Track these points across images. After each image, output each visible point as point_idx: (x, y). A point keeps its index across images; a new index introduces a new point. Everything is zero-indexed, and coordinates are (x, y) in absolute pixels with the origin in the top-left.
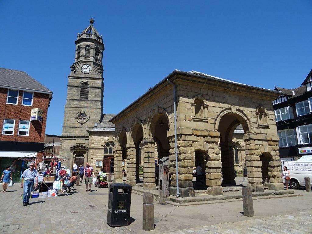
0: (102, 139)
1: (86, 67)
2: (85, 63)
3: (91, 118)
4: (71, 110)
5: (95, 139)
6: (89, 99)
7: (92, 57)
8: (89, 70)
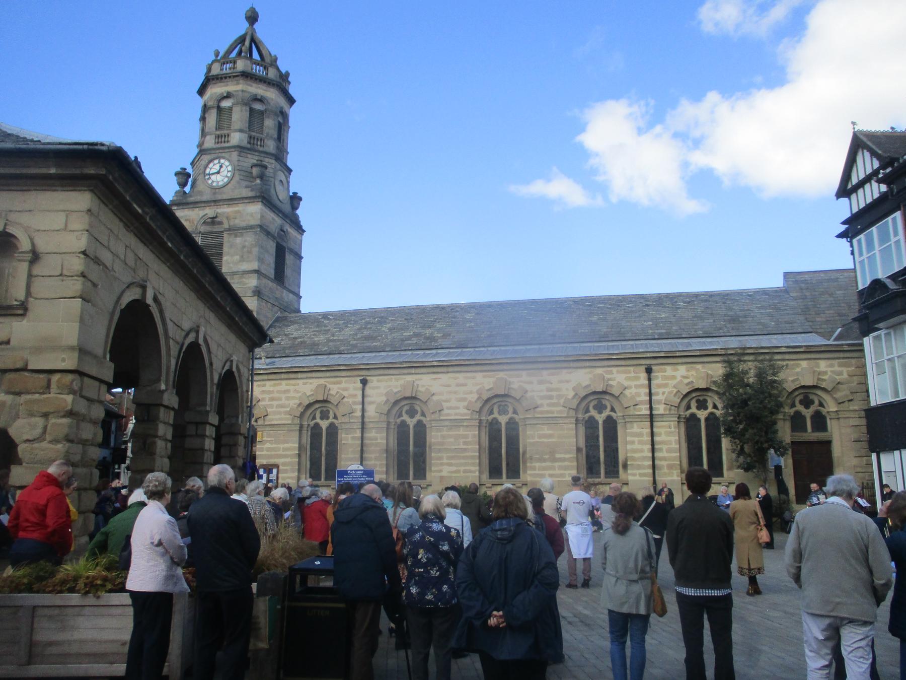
1: (217, 167)
2: (215, 156)
7: (236, 131)
8: (227, 176)
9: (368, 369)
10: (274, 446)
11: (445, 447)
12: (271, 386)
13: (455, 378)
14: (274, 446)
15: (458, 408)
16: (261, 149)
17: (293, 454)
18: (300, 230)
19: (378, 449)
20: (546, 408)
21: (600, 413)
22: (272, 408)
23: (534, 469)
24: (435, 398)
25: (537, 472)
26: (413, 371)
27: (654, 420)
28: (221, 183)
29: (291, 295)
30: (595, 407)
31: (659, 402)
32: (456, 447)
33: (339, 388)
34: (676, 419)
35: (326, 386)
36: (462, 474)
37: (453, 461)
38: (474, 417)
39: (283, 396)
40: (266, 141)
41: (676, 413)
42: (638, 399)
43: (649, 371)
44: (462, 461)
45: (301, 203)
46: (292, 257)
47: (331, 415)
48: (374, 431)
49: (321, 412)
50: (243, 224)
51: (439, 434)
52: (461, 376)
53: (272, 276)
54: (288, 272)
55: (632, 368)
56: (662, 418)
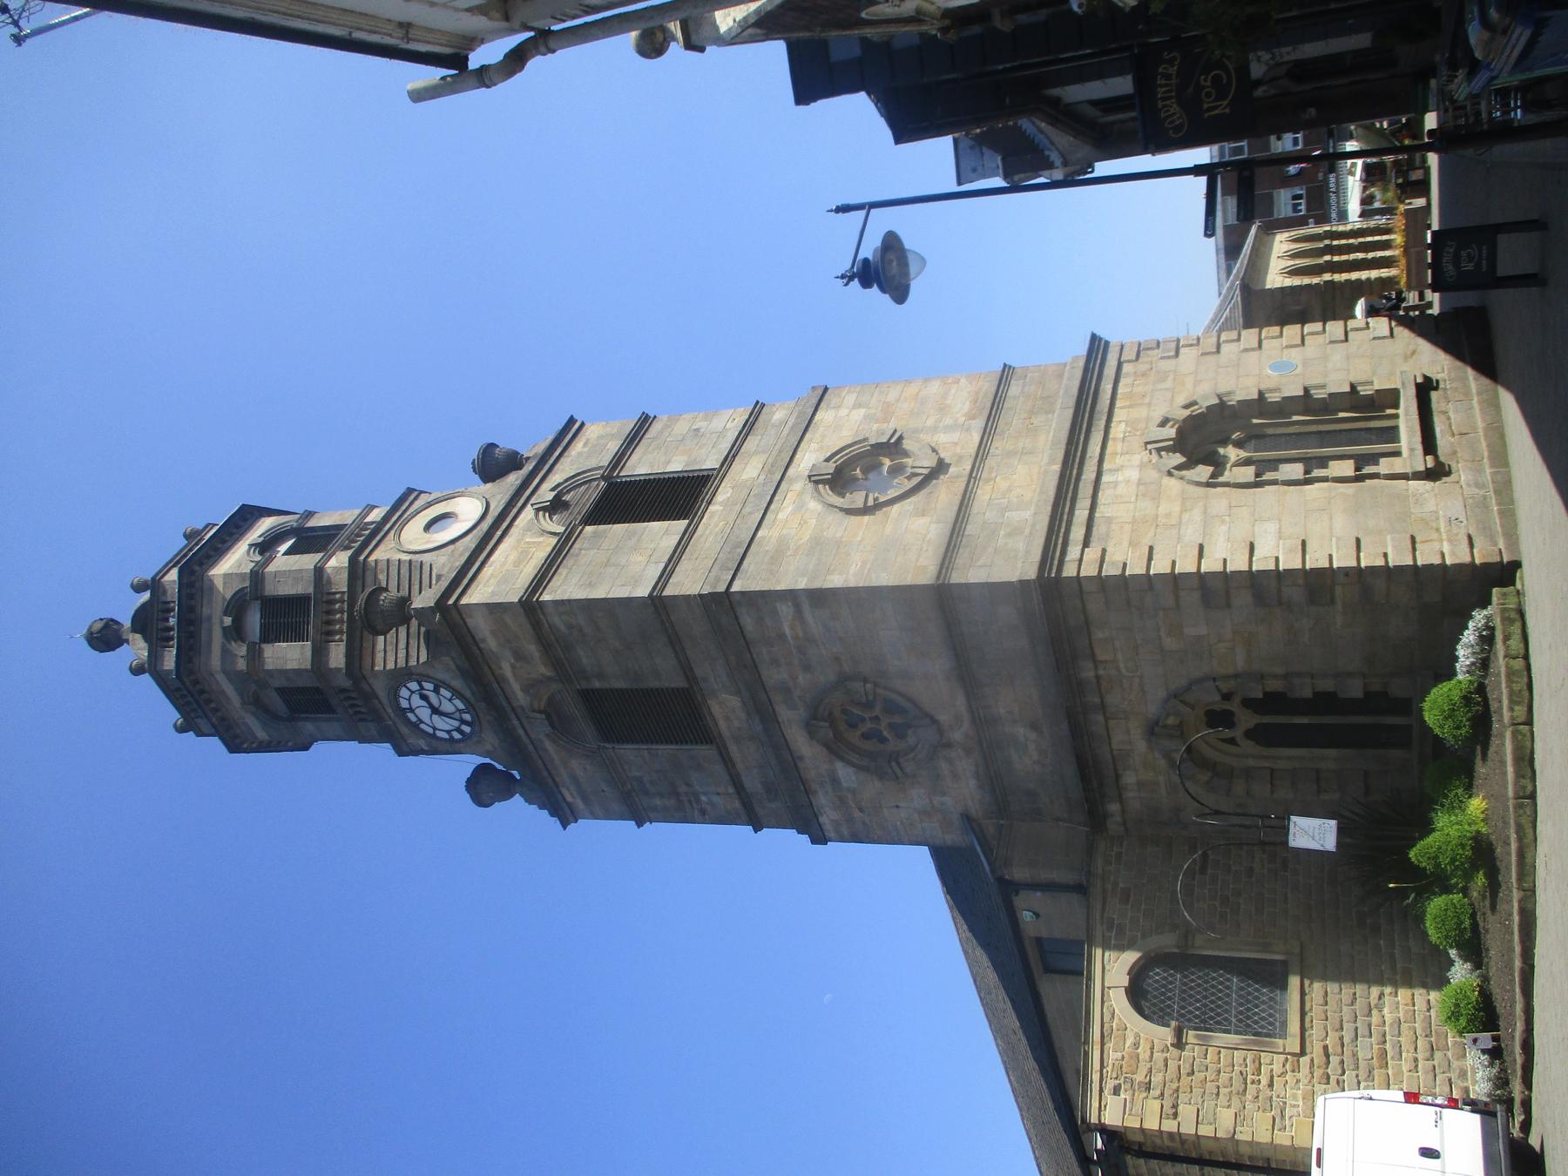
46: (635, 457)
53: (683, 523)
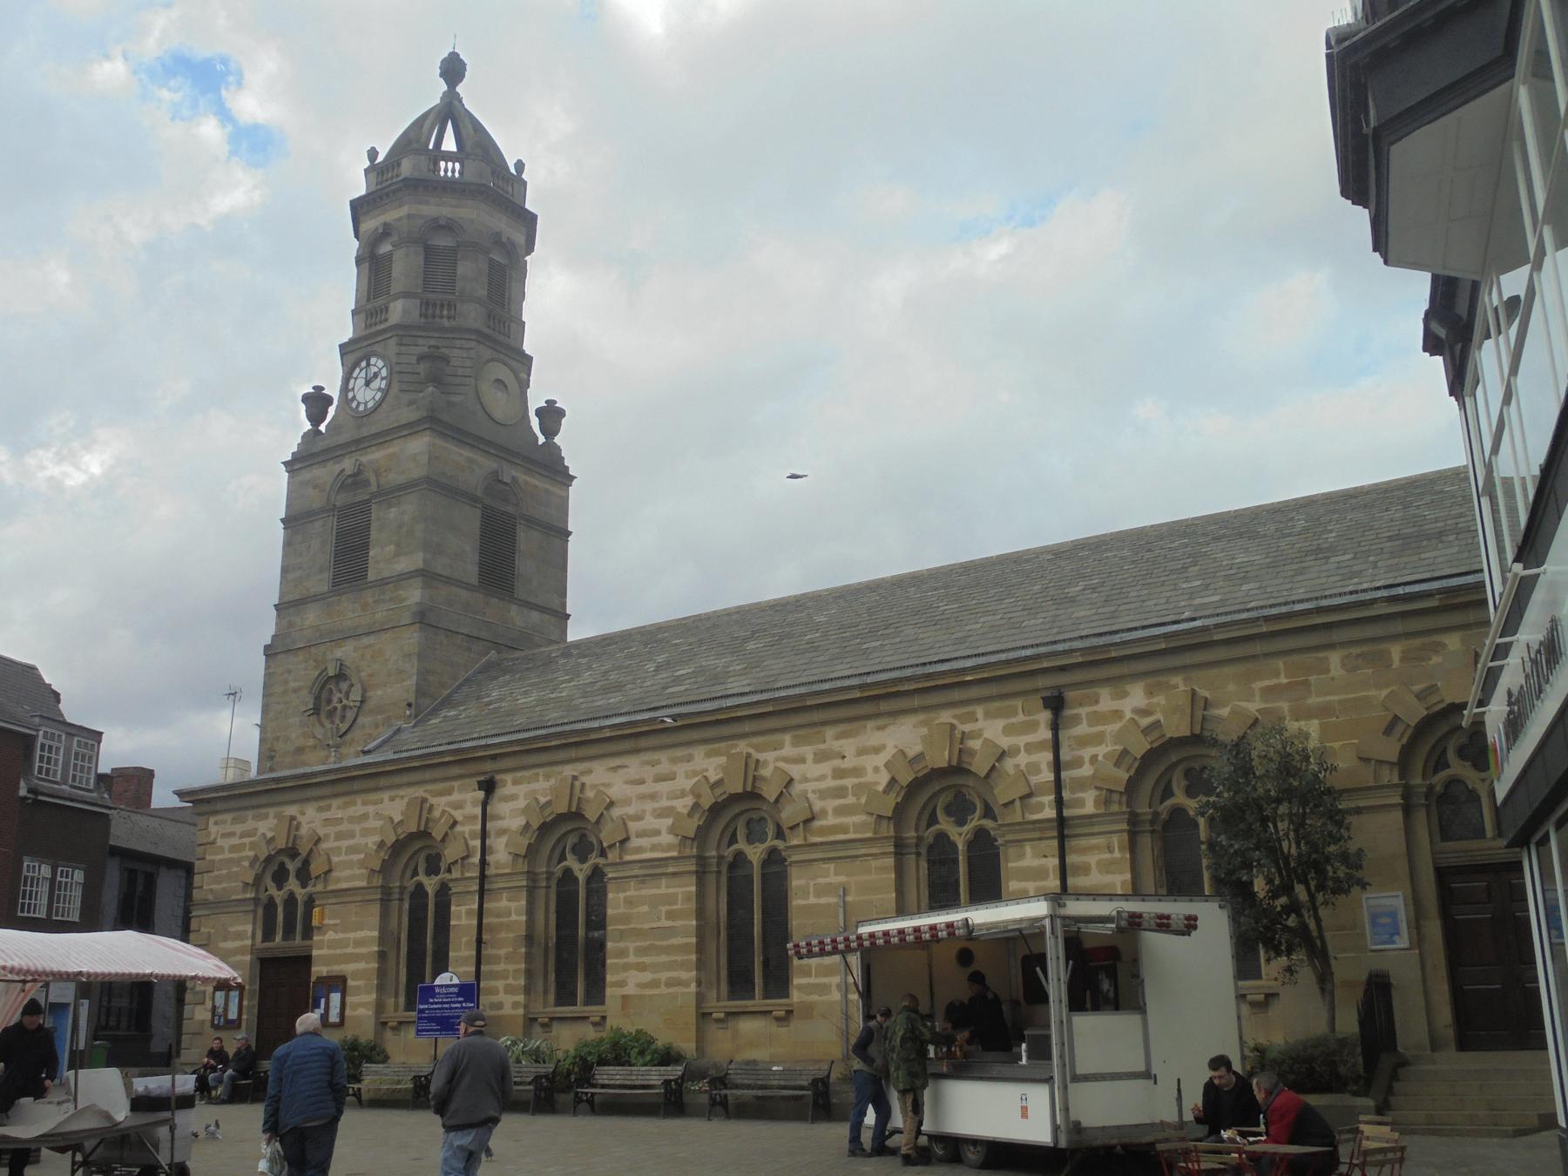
0: (247, 840)
3: (376, 695)
4: (289, 671)
5: (219, 842)
6: (371, 576)
7: (396, 297)
9: (494, 757)
10: (340, 936)
11: (632, 926)
12: (339, 808)
13: (653, 764)
14: (340, 936)
15: (657, 833)
16: (446, 323)
17: (369, 953)
18: (566, 478)
19: (511, 935)
20: (831, 820)
21: (961, 822)
22: (340, 855)
23: (807, 973)
24: (616, 812)
25: (812, 980)
26: (573, 753)
27: (1066, 832)
28: (370, 405)
29: (535, 616)
30: (948, 811)
31: (1081, 784)
32: (655, 925)
33: (448, 804)
34: (1125, 826)
35: (424, 800)
36: (664, 990)
37: (647, 960)
38: (688, 852)
39: (357, 828)
40: (458, 306)
41: (1124, 808)
42: (1034, 780)
43: (1056, 704)
44: (664, 958)
45: (564, 421)
47: (443, 867)
48: (504, 895)
49: (428, 858)
50: (402, 479)
51: (622, 895)
52: (663, 756)
53: (474, 580)
54: (524, 566)
55: (1018, 703)
56: (1092, 825)
